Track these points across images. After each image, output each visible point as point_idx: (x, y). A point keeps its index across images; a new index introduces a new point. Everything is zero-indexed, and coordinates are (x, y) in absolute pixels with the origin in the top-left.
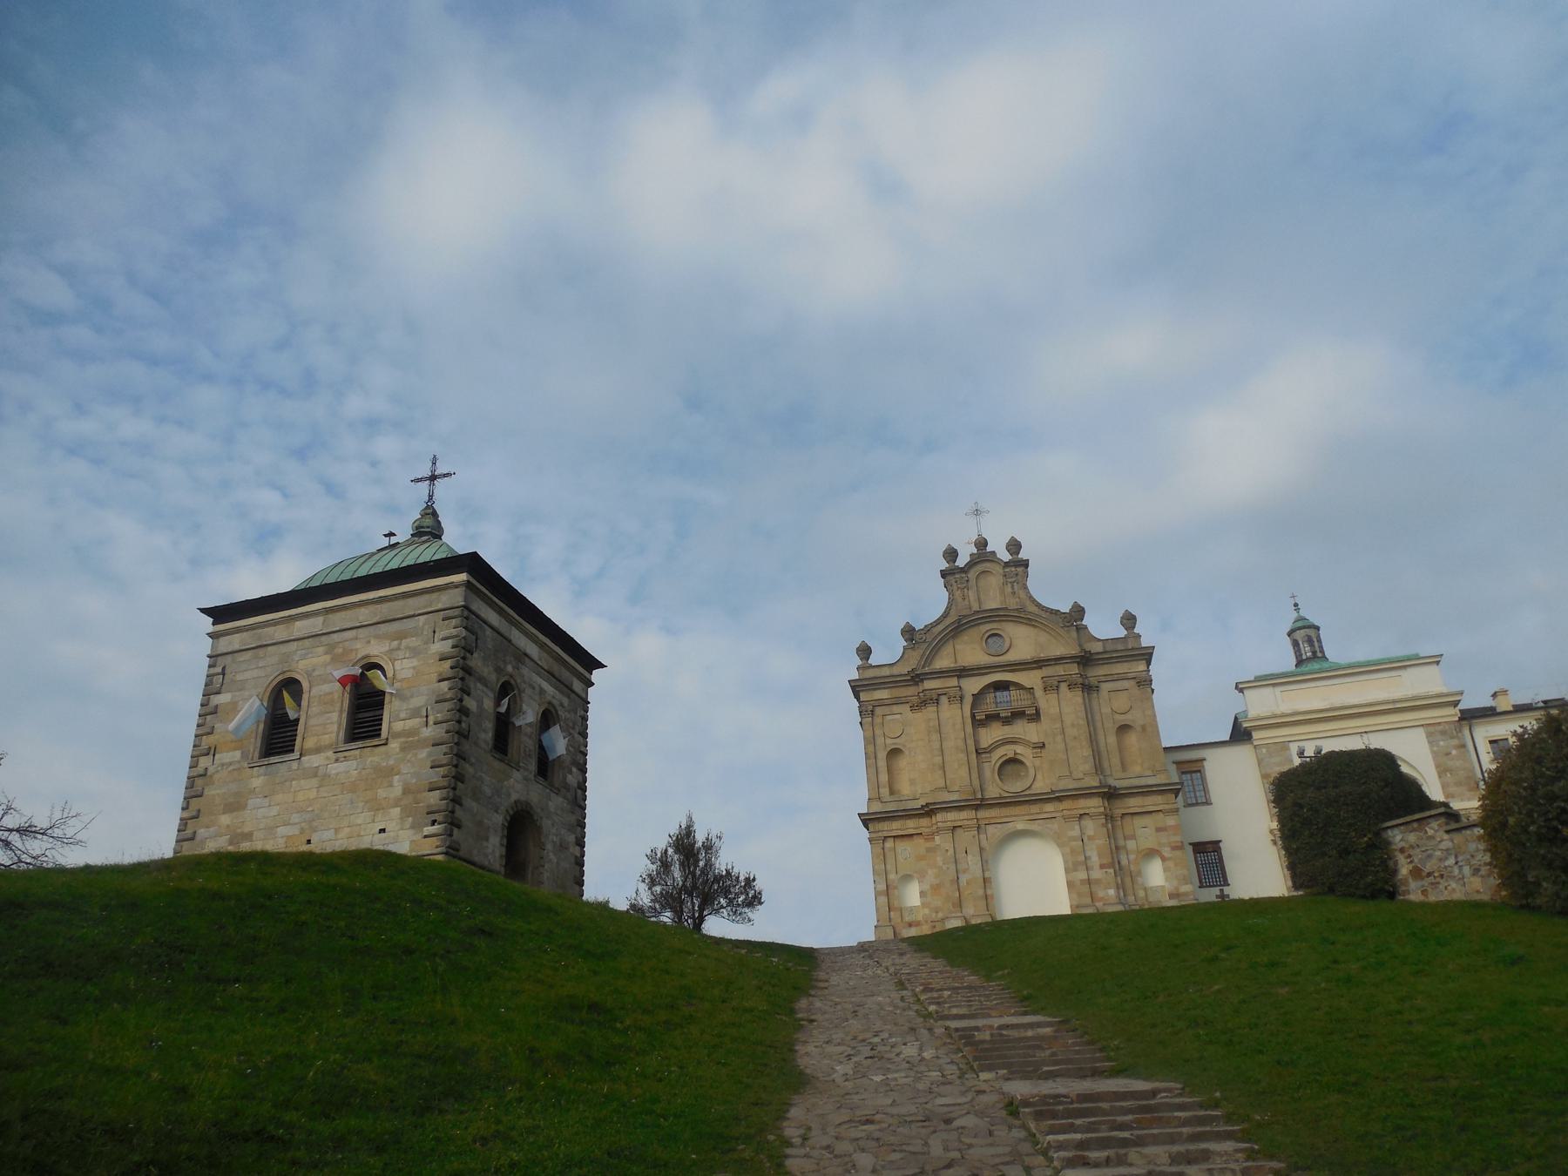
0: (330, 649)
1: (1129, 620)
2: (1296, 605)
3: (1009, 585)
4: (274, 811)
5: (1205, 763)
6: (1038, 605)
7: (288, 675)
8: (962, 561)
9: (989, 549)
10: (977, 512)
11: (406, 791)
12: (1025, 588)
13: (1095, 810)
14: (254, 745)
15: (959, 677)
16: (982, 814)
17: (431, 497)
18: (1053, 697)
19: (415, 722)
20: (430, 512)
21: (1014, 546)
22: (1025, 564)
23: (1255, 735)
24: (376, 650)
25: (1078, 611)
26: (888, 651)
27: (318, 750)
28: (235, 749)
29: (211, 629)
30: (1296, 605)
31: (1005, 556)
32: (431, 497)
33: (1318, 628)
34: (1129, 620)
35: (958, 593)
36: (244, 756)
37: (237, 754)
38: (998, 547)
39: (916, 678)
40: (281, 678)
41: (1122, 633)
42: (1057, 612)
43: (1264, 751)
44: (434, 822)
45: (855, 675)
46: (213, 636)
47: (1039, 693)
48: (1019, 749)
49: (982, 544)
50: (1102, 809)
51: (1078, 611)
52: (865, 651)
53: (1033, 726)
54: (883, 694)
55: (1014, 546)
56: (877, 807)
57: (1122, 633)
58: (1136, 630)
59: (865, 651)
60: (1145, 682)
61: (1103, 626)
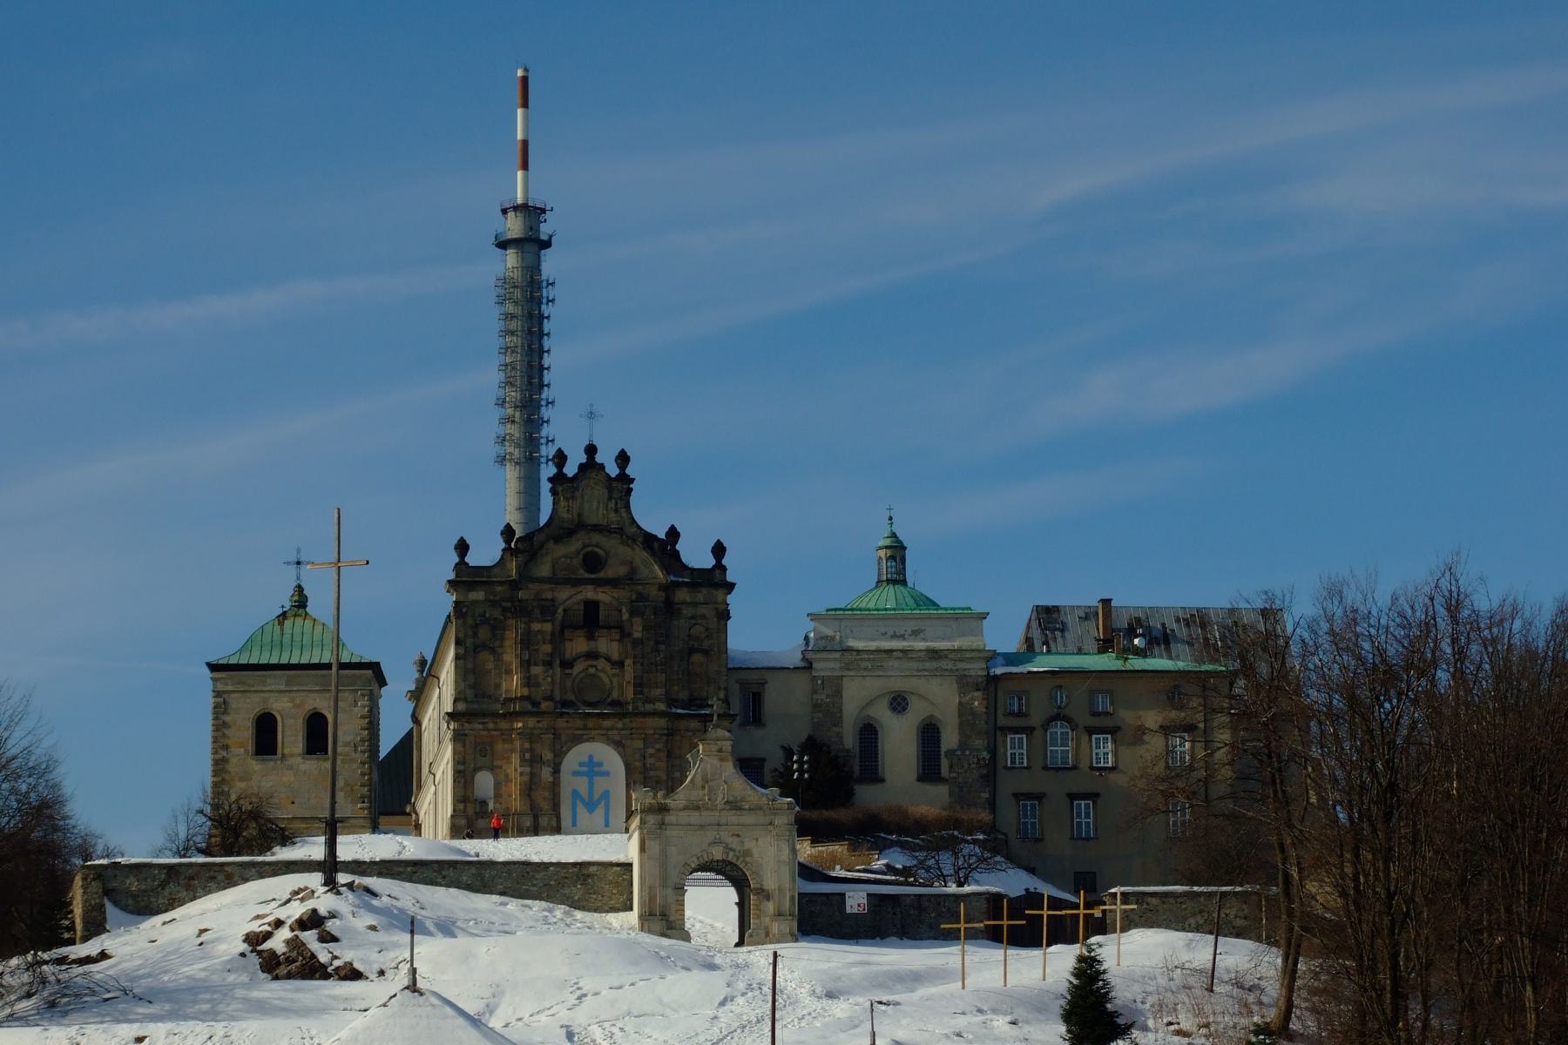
0: (292, 700)
1: (719, 550)
2: (891, 518)
3: (613, 501)
4: (271, 784)
5: (766, 686)
6: (639, 527)
7: (266, 711)
8: (570, 470)
9: (599, 458)
10: (591, 415)
11: (347, 784)
12: (627, 506)
13: (661, 732)
14: (251, 747)
15: (552, 590)
16: (561, 723)
17: (298, 578)
18: (637, 620)
19: (347, 749)
20: (300, 589)
21: (623, 459)
22: (632, 480)
23: (815, 665)
24: (323, 705)
25: (673, 534)
26: (487, 552)
27: (292, 756)
28: (240, 747)
29: (211, 676)
30: (891, 518)
31: (613, 470)
32: (298, 578)
33: (905, 548)
34: (719, 550)
35: (563, 503)
36: (246, 752)
37: (242, 750)
38: (606, 458)
39: (515, 585)
40: (263, 711)
41: (708, 562)
42: (655, 537)
43: (819, 682)
44: (363, 802)
45: (452, 576)
46: (212, 678)
47: (626, 616)
48: (601, 663)
49: (591, 450)
50: (666, 732)
51: (673, 534)
52: (462, 547)
53: (615, 645)
54: (478, 595)
55: (623, 459)
56: (461, 707)
57: (708, 562)
58: (724, 562)
59: (462, 547)
60: (725, 615)
61: (696, 555)
